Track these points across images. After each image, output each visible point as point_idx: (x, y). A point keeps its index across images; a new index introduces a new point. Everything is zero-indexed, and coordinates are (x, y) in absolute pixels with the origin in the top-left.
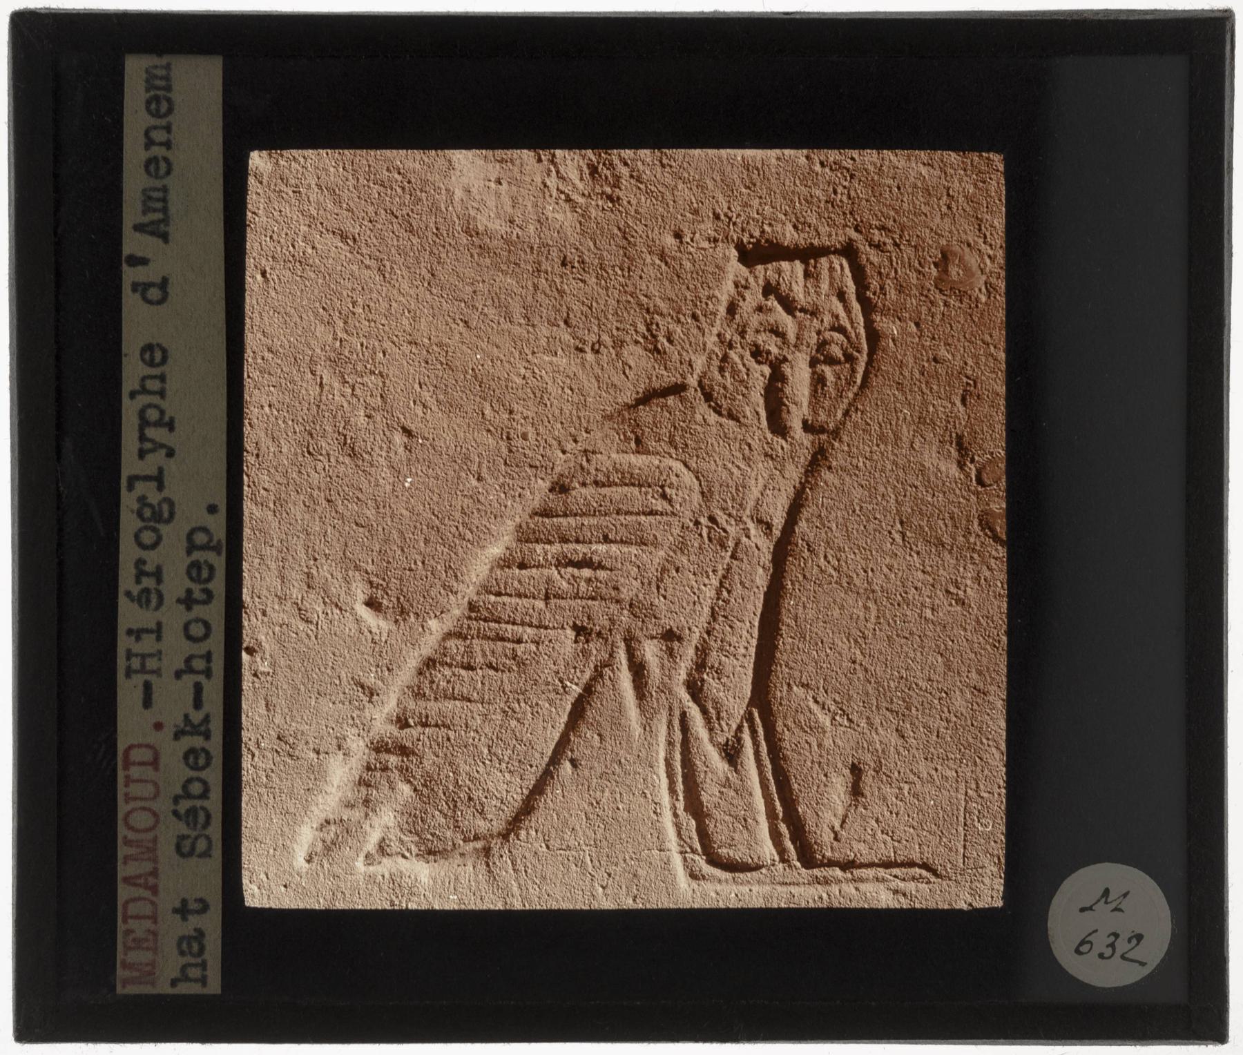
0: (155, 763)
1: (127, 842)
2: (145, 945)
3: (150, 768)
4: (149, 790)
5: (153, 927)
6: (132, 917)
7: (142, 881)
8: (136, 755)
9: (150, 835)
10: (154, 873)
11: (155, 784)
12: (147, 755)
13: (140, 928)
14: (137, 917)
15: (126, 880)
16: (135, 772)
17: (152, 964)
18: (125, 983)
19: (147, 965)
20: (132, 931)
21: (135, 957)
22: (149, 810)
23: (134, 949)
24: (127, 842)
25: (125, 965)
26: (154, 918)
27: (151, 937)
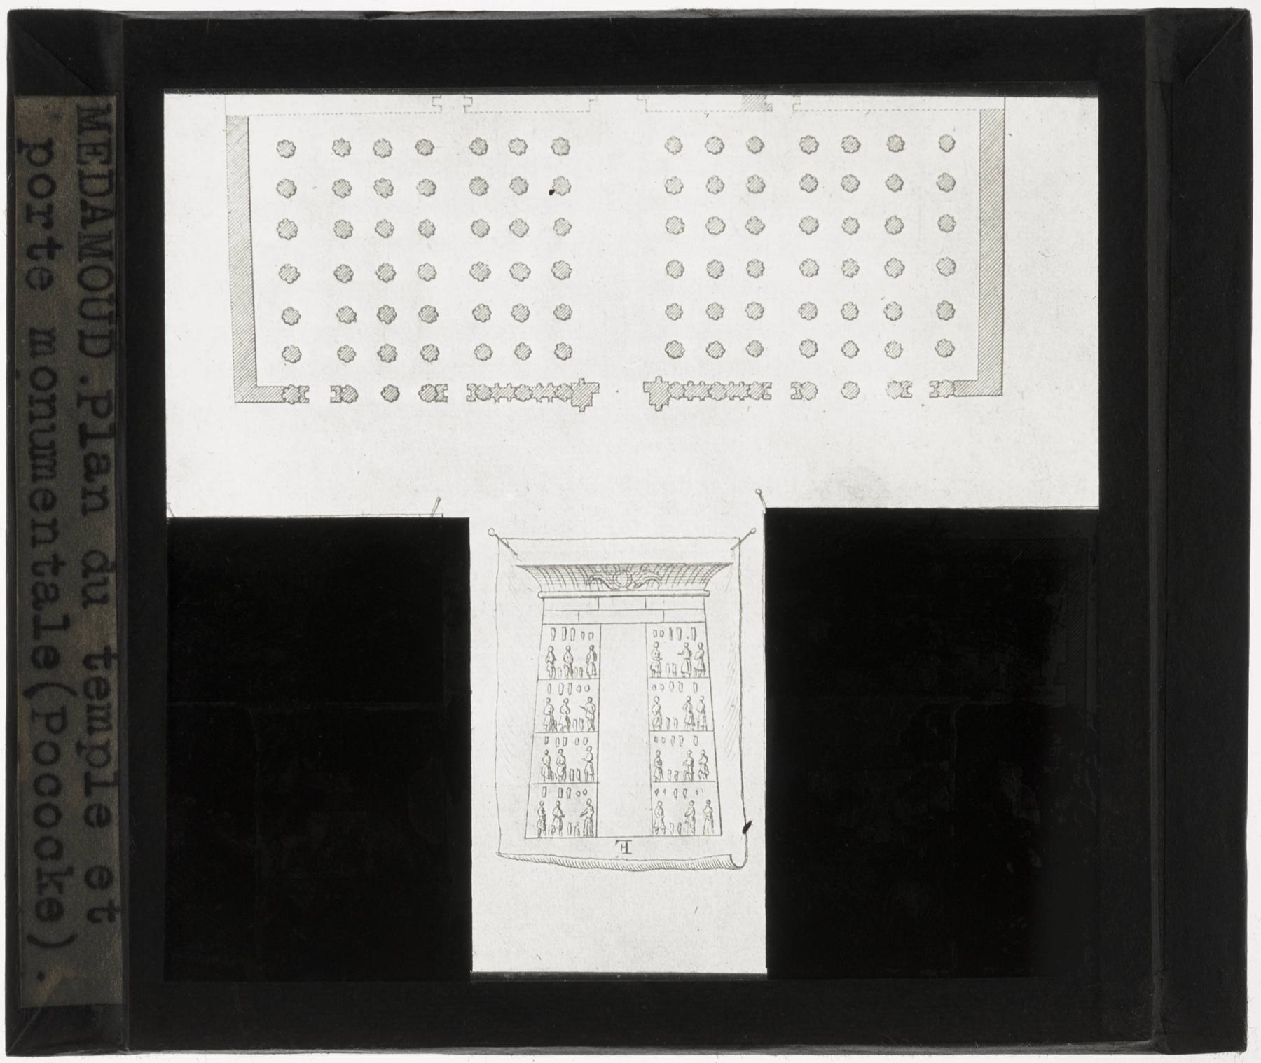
0: (82, 334)
1: (109, 254)
2: (90, 149)
3: (88, 333)
4: (91, 309)
5: (83, 167)
6: (104, 177)
7: (99, 214)
8: (104, 345)
9: (88, 262)
10: (85, 222)
11: (83, 315)
12: (91, 345)
13: (96, 166)
14: (98, 177)
15: (107, 214)
16: (102, 327)
17: (81, 130)
18: (108, 109)
19: (88, 129)
20: (102, 163)
21: (98, 136)
22: (87, 288)
23: (103, 144)
24: (109, 254)
25: (107, 126)
26: (82, 176)
27: (85, 157)
